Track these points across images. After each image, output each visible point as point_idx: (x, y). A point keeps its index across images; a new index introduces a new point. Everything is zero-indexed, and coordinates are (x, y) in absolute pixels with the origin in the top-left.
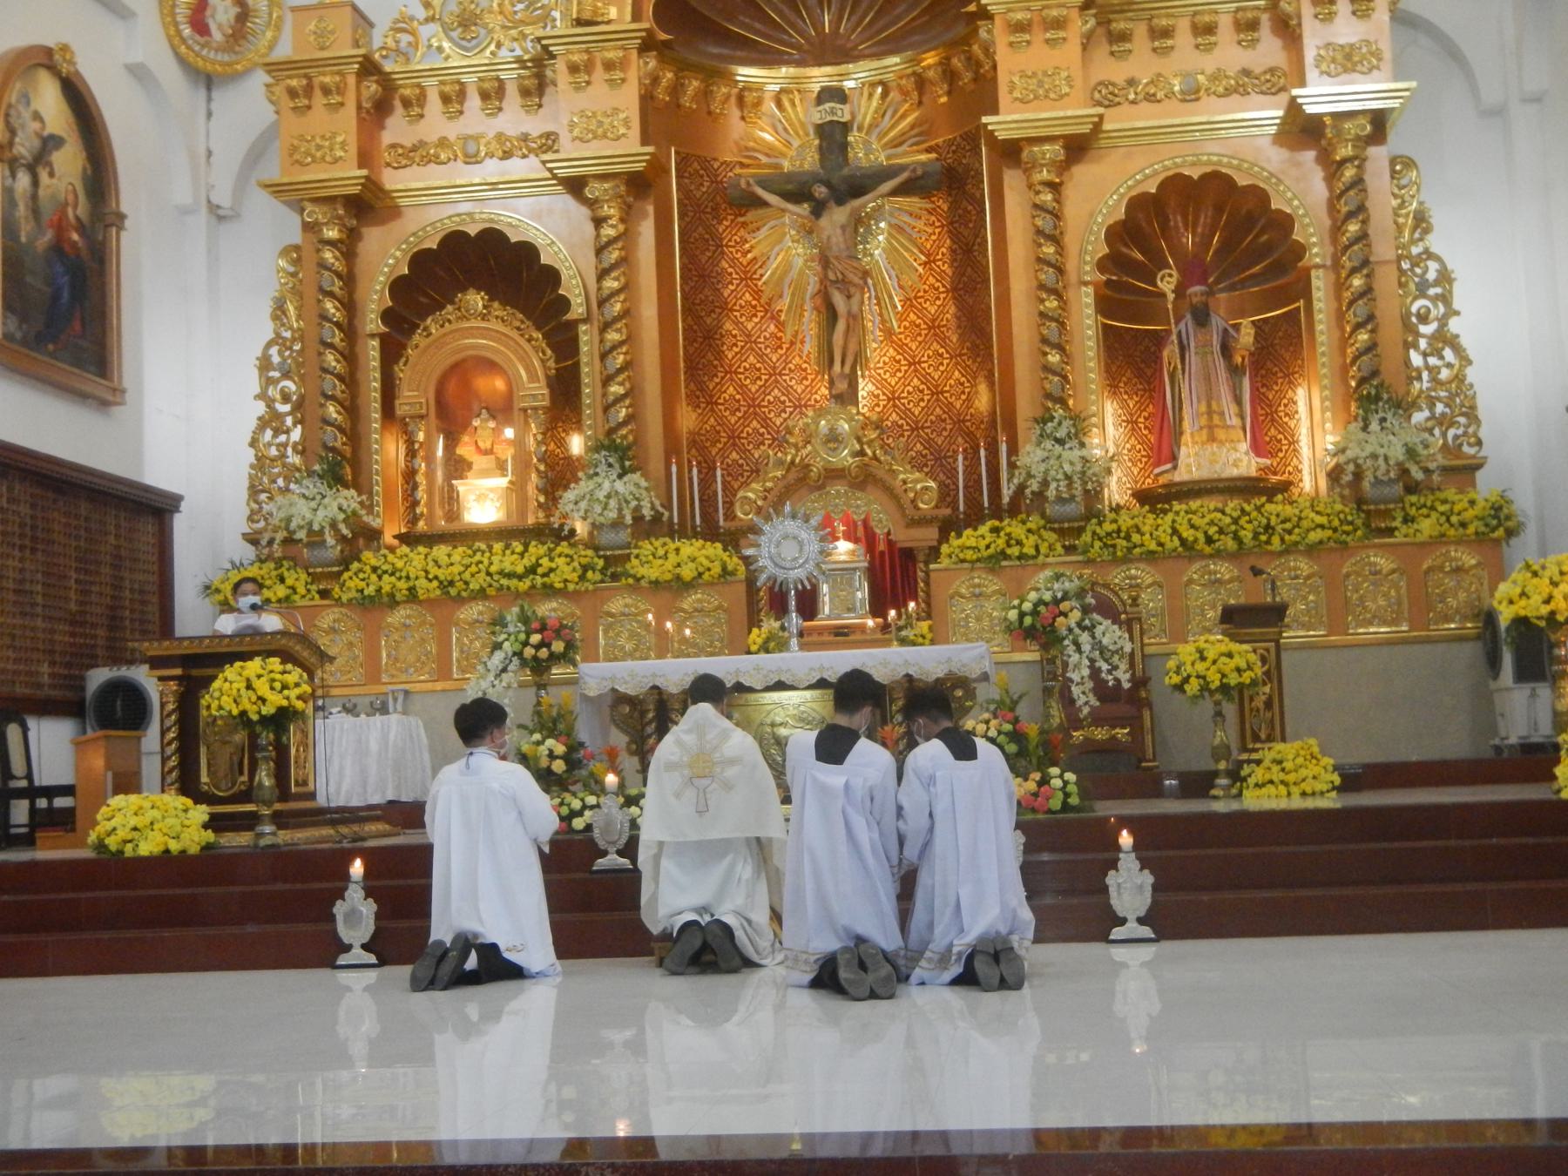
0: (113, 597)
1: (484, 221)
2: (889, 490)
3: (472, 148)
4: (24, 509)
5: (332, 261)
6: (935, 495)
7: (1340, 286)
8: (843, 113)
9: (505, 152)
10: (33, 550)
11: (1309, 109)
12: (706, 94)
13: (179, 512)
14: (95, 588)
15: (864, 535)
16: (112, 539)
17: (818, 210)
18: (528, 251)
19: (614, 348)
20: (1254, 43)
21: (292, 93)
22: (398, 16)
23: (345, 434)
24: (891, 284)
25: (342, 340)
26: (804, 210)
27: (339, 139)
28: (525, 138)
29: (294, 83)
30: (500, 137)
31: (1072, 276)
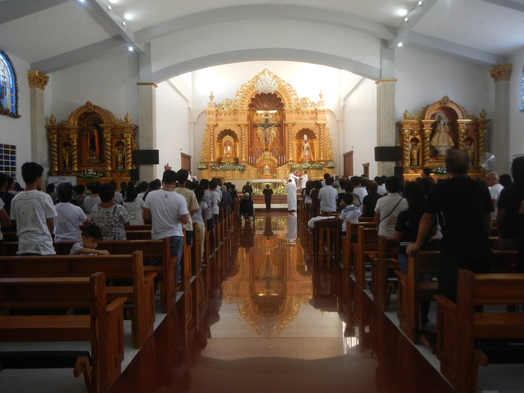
2: (273, 161)
6: (277, 161)
7: (320, 141)
8: (268, 117)
11: (318, 123)
12: (253, 114)
15: (270, 166)
17: (265, 128)
18: (233, 132)
19: (243, 143)
20: (312, 114)
21: (208, 113)
24: (273, 137)
26: (263, 128)
28: (233, 119)
31: (292, 138)
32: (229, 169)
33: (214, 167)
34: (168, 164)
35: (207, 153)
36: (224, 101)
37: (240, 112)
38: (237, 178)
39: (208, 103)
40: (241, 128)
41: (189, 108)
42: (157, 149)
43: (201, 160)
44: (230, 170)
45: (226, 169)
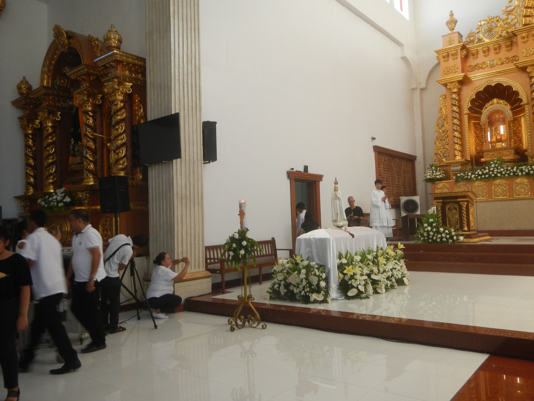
0: (404, 181)
1: (496, 82)
3: (492, 63)
4: (387, 162)
5: (455, 97)
9: (501, 63)
10: (389, 171)
13: (416, 160)
14: (400, 179)
16: (403, 168)
18: (509, 88)
21: (444, 57)
22: (469, 33)
23: (460, 139)
25: (458, 116)
27: (456, 67)
28: (507, 59)
29: (444, 54)
30: (500, 59)
32: (499, 175)
33: (462, 174)
34: (306, 168)
35: (448, 145)
36: (481, 26)
37: (524, 35)
38: (522, 196)
39: (443, 36)
40: (529, 73)
41: (404, 59)
42: (173, 113)
43: (435, 161)
44: (503, 177)
45: (493, 175)
